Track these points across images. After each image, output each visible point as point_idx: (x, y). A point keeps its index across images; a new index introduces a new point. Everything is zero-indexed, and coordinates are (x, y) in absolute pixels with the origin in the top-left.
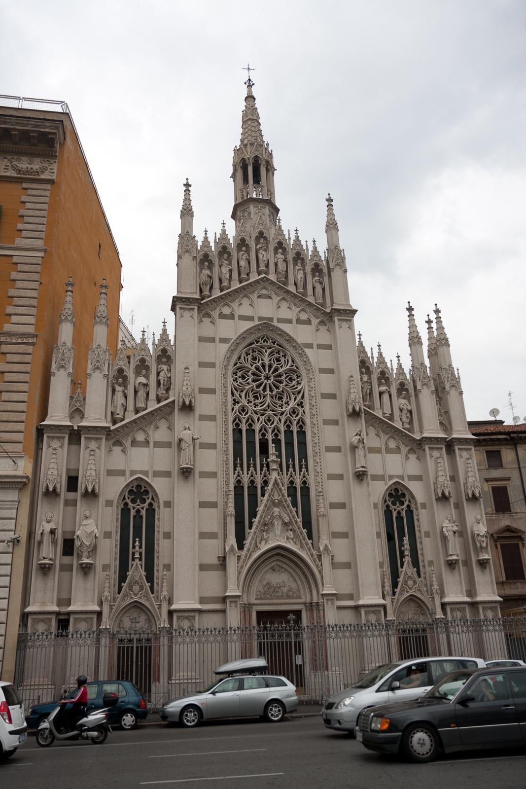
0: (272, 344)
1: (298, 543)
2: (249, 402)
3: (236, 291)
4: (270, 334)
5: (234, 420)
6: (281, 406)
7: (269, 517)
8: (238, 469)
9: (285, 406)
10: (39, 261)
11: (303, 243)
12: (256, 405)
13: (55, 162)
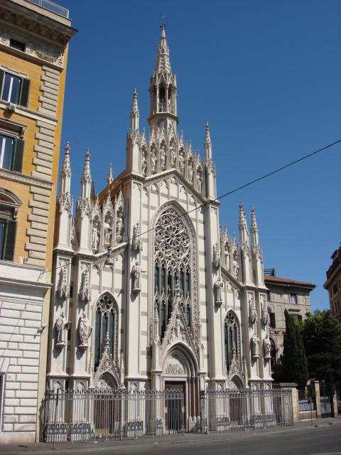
2: (163, 250)
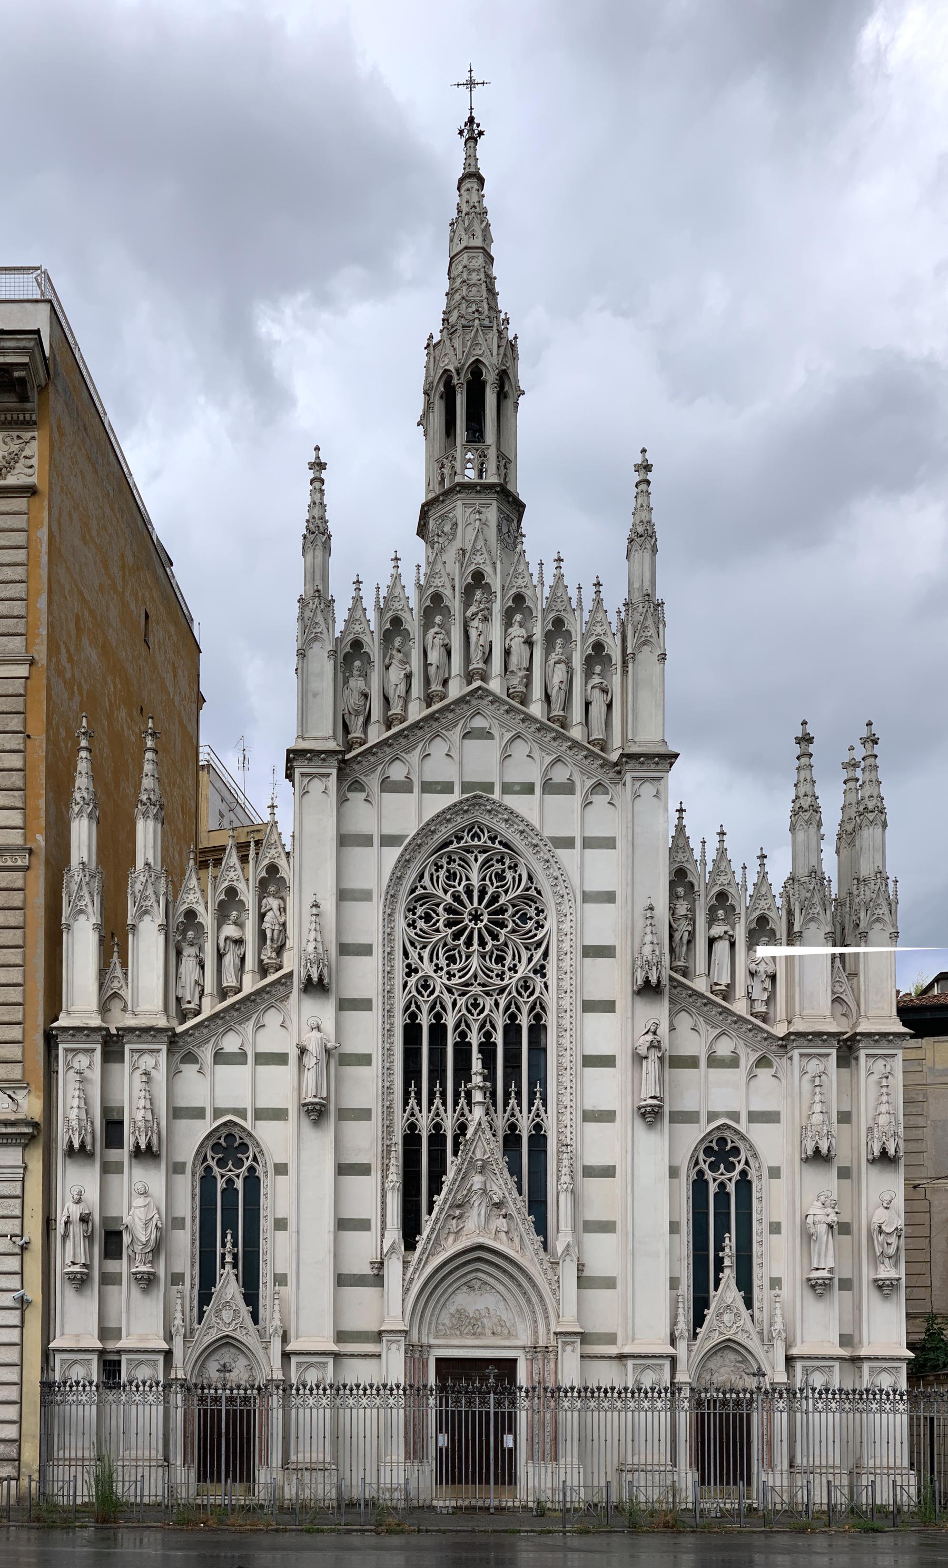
0: (489, 843)
1: (517, 1240)
2: (438, 969)
3: (416, 726)
4: (486, 819)
5: (407, 1007)
6: (501, 976)
7: (465, 1192)
8: (412, 1101)
9: (508, 974)
10: (18, 687)
11: (572, 593)
12: (450, 976)
13: (33, 438)
